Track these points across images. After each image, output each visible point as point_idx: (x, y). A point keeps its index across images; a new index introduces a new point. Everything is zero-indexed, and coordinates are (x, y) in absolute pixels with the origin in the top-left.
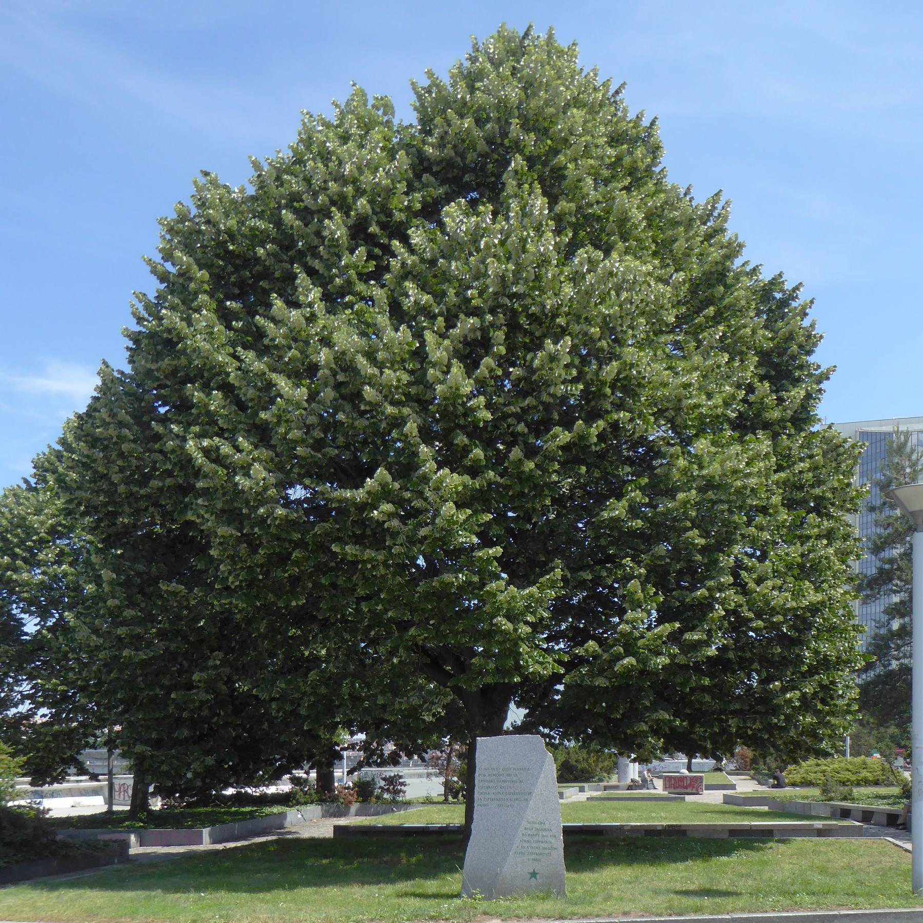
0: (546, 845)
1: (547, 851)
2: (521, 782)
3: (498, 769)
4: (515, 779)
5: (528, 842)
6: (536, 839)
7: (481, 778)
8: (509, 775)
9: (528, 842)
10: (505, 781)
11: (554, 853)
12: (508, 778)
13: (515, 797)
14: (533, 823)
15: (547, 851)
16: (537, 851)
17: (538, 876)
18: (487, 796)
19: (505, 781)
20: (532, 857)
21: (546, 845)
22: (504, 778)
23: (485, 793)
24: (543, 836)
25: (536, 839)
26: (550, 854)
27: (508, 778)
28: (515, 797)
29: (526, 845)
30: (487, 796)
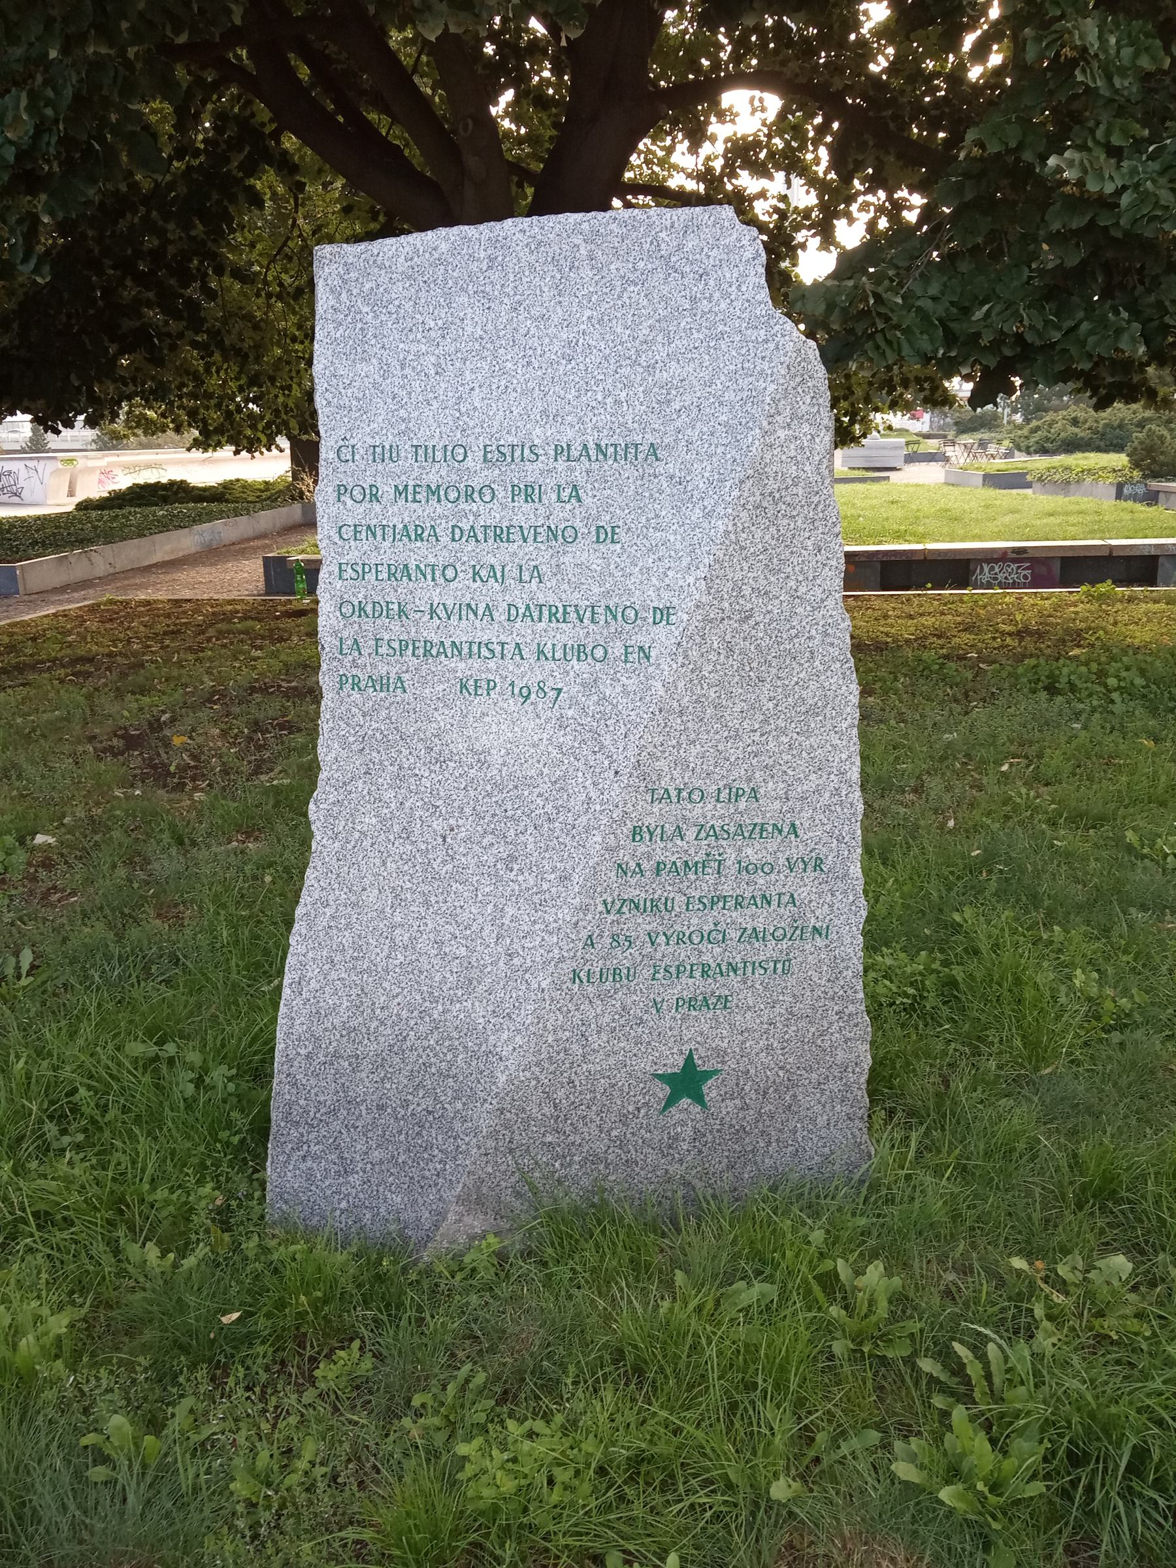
0: (761, 919)
1: (768, 951)
2: (606, 535)
3: (454, 454)
4: (560, 515)
5: (655, 907)
6: (705, 886)
7: (354, 512)
8: (529, 493)
9: (655, 907)
10: (500, 534)
11: (810, 952)
12: (524, 514)
13: (567, 634)
14: (685, 794)
15: (768, 951)
16: (711, 954)
17: (710, 1089)
18: (394, 630)
19: (500, 534)
20: (687, 986)
21: (761, 919)
22: (491, 514)
23: (381, 610)
24: (745, 868)
25: (705, 886)
26: (784, 966)
27: (524, 514)
28: (567, 634)
29: (643, 924)
30: (394, 630)
